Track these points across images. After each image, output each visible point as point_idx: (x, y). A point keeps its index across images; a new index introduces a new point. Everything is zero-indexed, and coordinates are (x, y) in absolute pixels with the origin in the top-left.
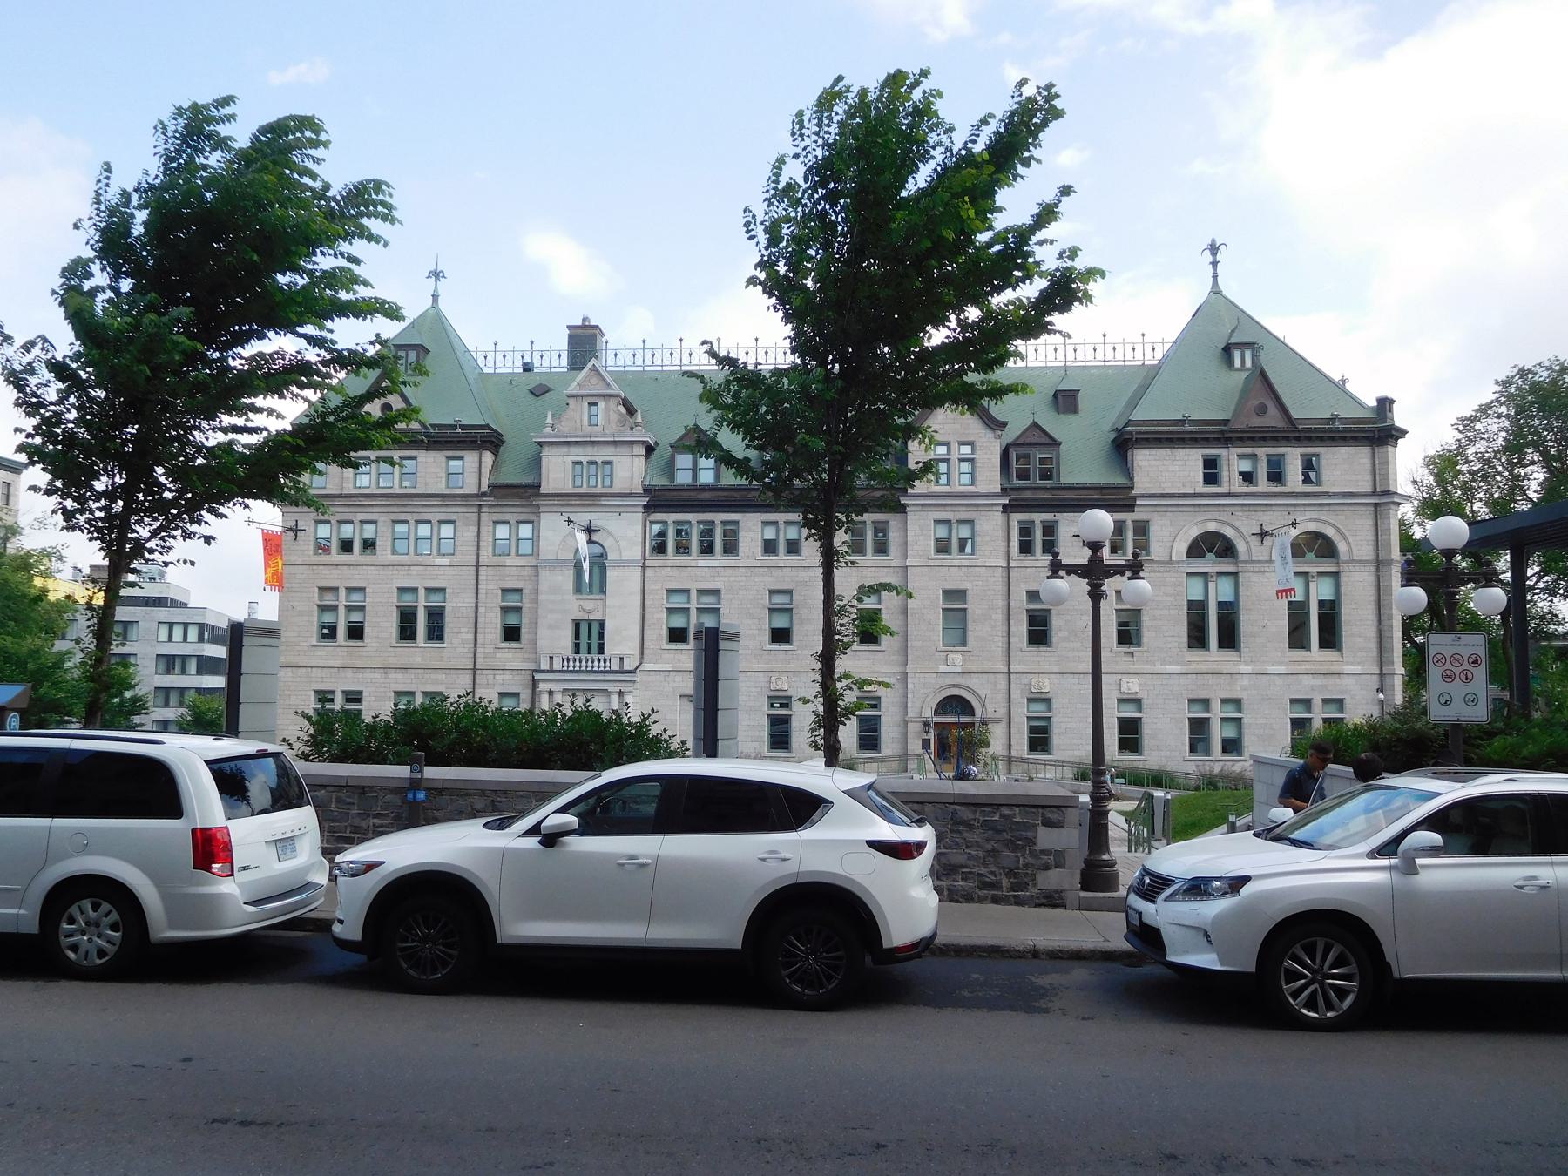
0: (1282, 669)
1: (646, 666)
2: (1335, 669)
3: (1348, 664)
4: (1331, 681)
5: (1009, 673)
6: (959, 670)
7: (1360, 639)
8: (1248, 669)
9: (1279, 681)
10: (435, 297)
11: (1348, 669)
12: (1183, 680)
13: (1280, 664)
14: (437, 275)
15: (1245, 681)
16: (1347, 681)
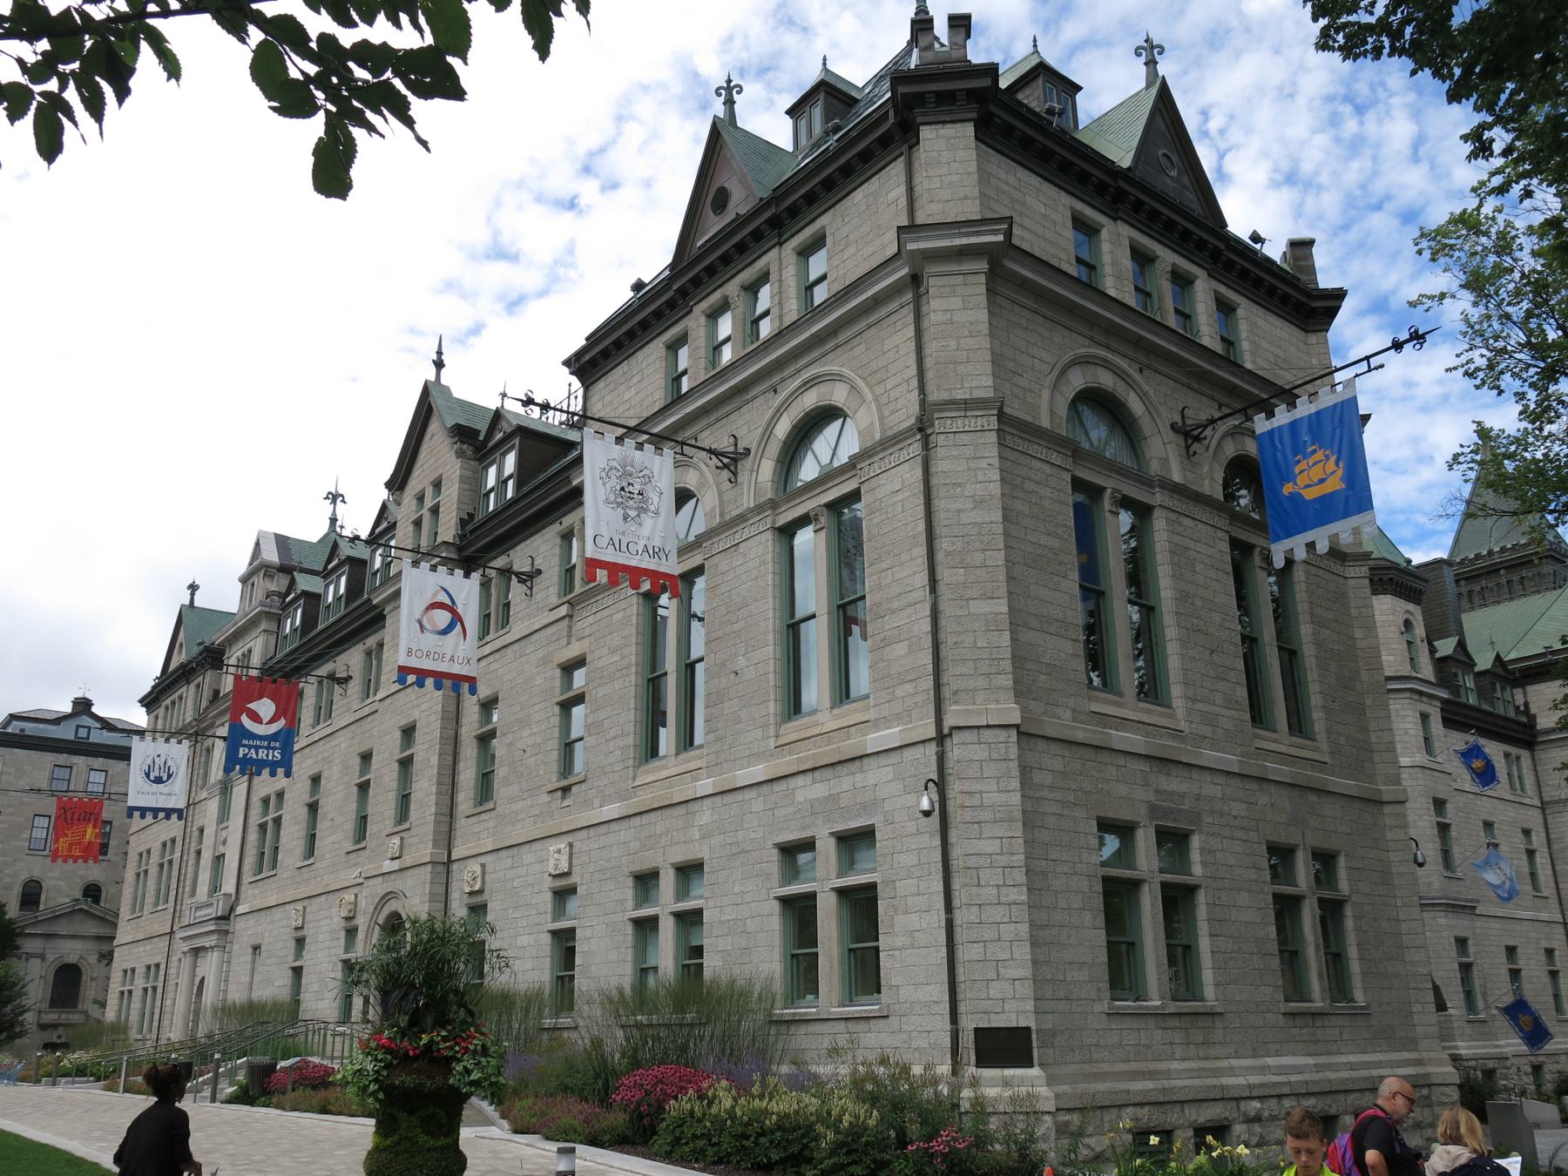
0: (758, 772)
1: (240, 910)
2: (849, 746)
3: (876, 724)
4: (845, 782)
5: (450, 861)
6: (396, 865)
7: (900, 649)
8: (705, 785)
9: (756, 802)
10: (333, 520)
11: (877, 739)
12: (624, 833)
13: (756, 757)
14: (334, 497)
15: (705, 816)
16: (877, 775)
